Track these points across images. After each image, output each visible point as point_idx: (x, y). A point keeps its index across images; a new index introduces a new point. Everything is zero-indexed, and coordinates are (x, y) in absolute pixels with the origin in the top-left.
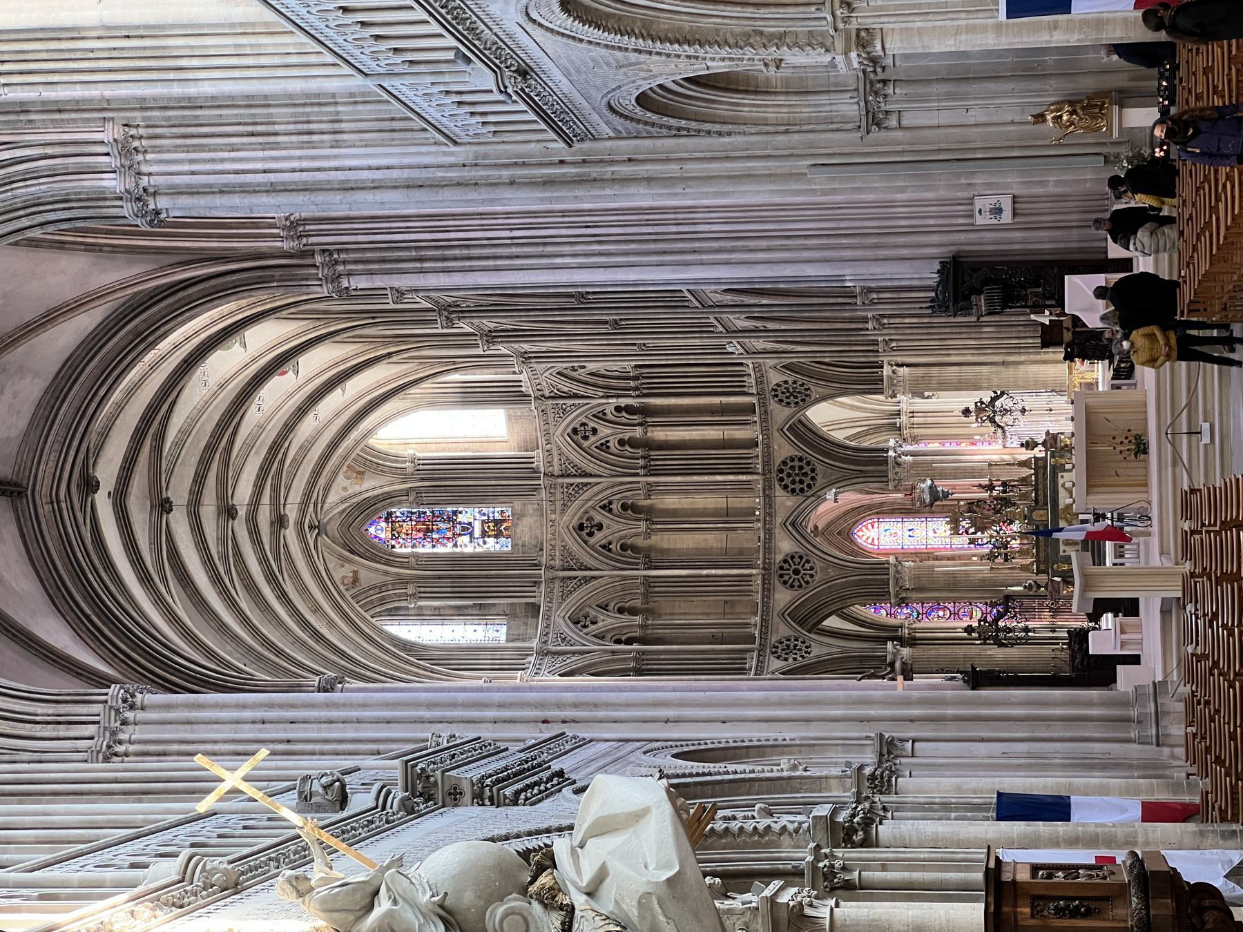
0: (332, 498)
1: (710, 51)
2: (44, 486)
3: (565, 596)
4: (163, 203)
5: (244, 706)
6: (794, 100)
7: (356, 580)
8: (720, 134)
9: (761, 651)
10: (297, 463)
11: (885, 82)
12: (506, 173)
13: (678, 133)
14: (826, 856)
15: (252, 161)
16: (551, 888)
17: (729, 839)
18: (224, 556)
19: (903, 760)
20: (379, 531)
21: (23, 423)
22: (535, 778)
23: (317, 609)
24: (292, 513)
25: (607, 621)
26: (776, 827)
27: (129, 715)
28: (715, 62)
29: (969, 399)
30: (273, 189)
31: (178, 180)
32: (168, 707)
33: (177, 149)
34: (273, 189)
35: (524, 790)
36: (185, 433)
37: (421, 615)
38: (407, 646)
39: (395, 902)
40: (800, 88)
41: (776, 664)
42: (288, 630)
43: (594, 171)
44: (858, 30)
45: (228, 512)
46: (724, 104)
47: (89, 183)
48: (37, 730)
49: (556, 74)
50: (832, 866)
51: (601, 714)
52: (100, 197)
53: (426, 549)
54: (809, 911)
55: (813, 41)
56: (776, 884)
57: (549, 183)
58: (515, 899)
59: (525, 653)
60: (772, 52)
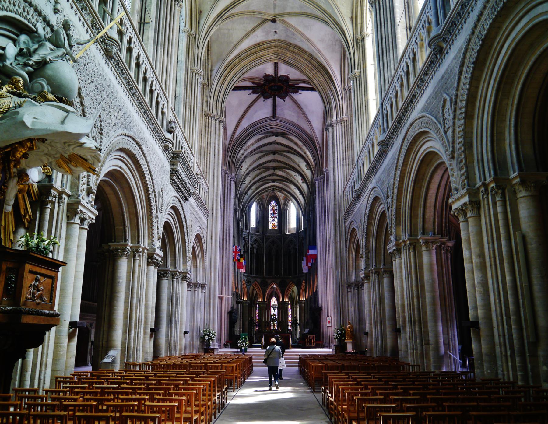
0: (279, 193)
1: (364, 241)
2: (274, 122)
3: (260, 238)
4: (330, 130)
5: (219, 145)
6: (354, 267)
7: (264, 198)
8: (346, 250)
9: (248, 276)
10: (285, 185)
11: (358, 288)
12: (337, 203)
13: (346, 240)
14: (144, 251)
15: (339, 148)
16: (46, 97)
17: (150, 226)
18: (265, 167)
19: (200, 289)
20: (273, 203)
21: (288, 118)
22: (183, 190)
23: (257, 189)
24: (276, 184)
25: (255, 246)
26: (154, 239)
27: (217, 121)
28: (363, 251)
29: (298, 318)
30: (334, 153)
31: (335, 132)
32: (219, 130)
33: (342, 132)
34: (334, 153)
35: (176, 183)
36: (289, 158)
37: (257, 211)
38: (250, 208)
39: (52, 50)
40: (357, 267)
41: (246, 279)
42: (251, 181)
43: (338, 223)
44: (369, 276)
45: (274, 168)
46: (353, 250)
47: (334, 114)
48: (215, 102)
49: (359, 205)
50: (141, 252)
51: (214, 222)
52: (332, 117)
53: (270, 213)
54: (77, 217)
55: (367, 265)
56: (96, 212)
57: (335, 213)
58: (48, 89)
59: (249, 230)
60: (364, 256)
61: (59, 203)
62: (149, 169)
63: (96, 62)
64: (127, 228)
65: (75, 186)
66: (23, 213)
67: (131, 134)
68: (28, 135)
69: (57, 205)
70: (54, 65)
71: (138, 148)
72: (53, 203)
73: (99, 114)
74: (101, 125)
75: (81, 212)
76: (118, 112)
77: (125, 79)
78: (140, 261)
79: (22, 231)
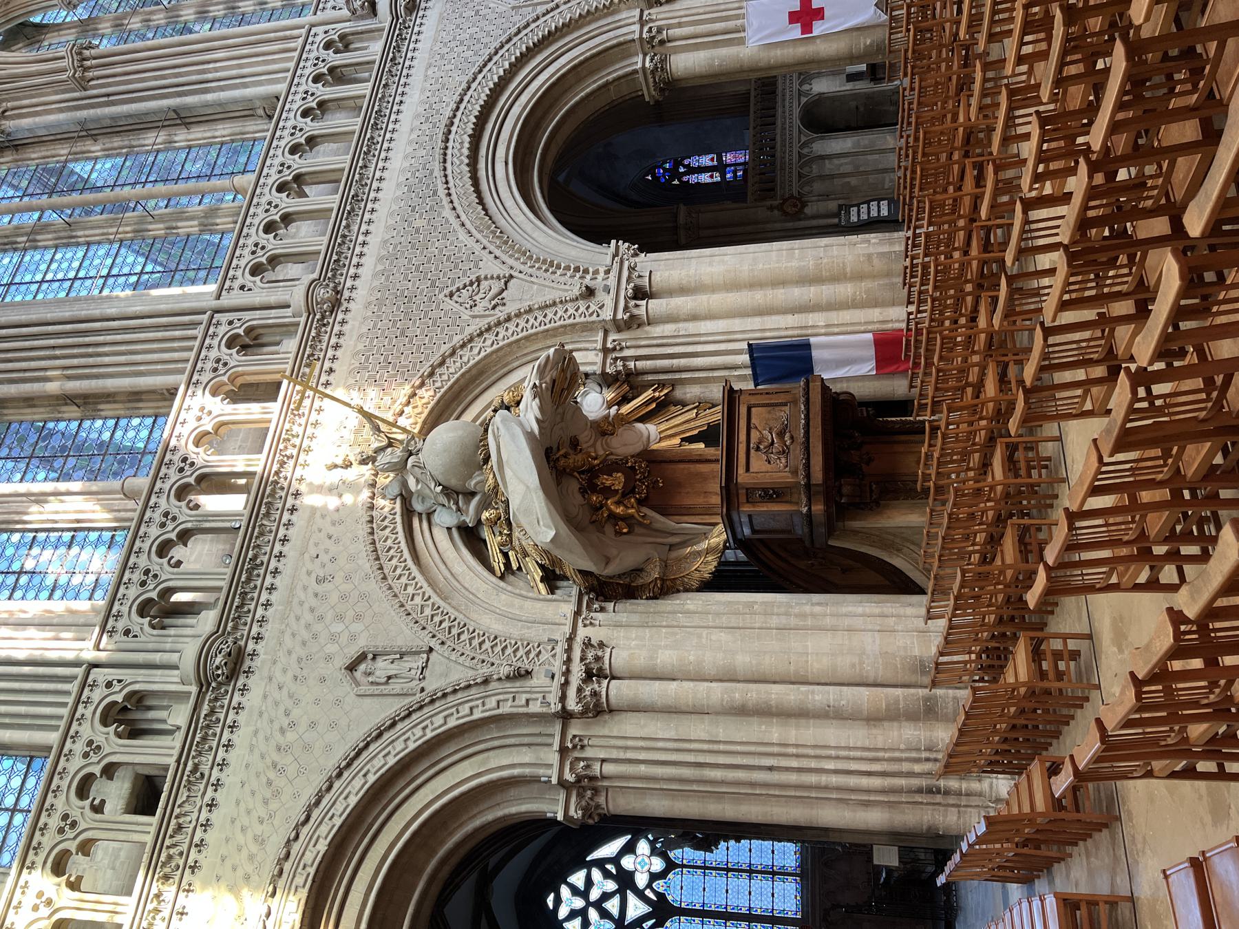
54: (636, 311)
61: (622, 349)
62: (480, 71)
63: (365, 330)
64: (610, 78)
65: (587, 328)
66: (654, 405)
67: (437, 167)
68: (564, 530)
69: (627, 353)
70: (440, 478)
71: (454, 129)
72: (624, 359)
73: (447, 299)
74: (465, 286)
75: (626, 308)
76: (417, 231)
77: (348, 226)
78: (669, 27)
79: (679, 393)
